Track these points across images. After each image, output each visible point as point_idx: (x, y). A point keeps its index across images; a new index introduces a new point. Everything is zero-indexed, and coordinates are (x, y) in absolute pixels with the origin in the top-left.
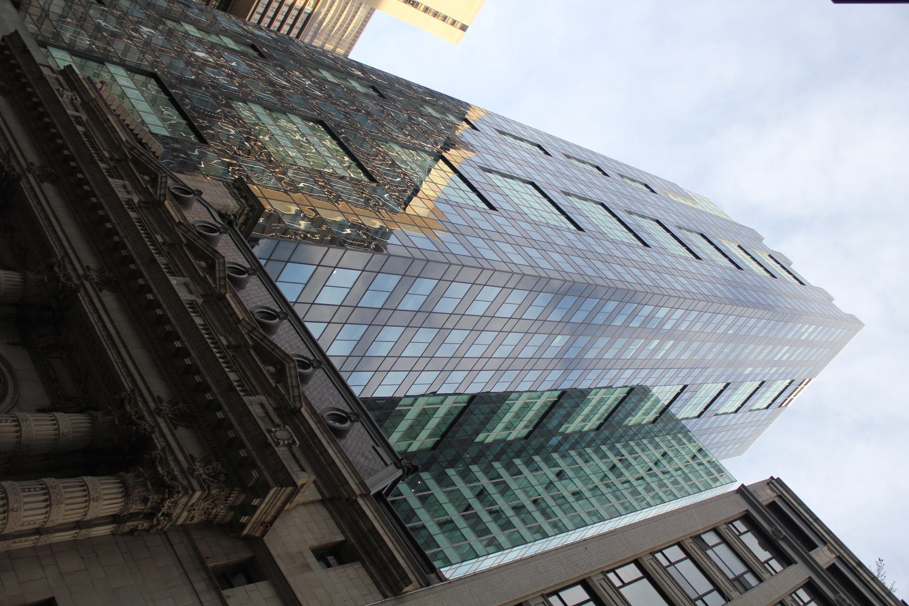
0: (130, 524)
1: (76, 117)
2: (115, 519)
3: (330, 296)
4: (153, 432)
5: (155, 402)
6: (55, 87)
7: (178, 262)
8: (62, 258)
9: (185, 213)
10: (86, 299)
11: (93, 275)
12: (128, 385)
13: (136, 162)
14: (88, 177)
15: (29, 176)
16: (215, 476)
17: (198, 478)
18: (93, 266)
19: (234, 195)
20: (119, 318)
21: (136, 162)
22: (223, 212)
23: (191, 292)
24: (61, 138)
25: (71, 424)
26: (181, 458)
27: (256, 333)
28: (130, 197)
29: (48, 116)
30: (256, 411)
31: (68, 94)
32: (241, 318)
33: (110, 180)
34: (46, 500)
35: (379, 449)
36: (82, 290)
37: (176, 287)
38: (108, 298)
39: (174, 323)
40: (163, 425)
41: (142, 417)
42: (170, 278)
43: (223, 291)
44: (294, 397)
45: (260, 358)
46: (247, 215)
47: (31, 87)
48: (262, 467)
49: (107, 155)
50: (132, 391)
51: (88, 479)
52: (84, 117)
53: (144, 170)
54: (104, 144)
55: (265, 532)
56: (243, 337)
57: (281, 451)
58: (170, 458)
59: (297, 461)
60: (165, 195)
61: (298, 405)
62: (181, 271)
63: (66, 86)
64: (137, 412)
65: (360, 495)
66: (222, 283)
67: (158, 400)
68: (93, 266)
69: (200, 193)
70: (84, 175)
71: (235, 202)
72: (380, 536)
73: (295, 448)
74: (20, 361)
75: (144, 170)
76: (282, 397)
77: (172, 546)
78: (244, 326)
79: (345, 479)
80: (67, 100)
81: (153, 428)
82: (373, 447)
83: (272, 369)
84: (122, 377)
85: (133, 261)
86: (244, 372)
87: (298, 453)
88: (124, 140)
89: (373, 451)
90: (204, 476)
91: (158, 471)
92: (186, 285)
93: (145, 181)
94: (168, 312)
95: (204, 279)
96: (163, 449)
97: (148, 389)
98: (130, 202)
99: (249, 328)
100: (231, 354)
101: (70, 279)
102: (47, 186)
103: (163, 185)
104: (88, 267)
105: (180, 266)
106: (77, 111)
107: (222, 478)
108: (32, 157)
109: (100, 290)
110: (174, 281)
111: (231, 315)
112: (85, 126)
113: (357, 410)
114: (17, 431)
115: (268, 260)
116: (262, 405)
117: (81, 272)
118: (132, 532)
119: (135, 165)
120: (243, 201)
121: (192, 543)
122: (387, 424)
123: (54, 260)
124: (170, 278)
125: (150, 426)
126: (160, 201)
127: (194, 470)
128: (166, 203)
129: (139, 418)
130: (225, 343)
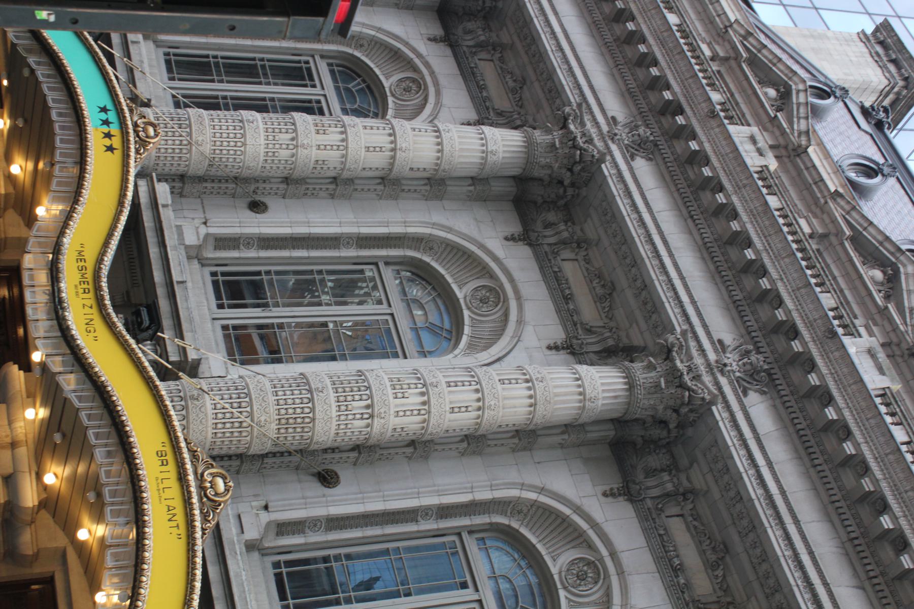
7: (836, 273)
10: (725, 415)
11: (732, 359)
13: (753, 62)
15: (614, 147)
18: (729, 339)
19: (875, 56)
20: (779, 450)
21: (753, 62)
23: (881, 371)
29: (633, 18)
33: (732, 129)
37: (856, 361)
38: (760, 409)
39: (879, 475)
46: (898, 93)
53: (767, 77)
54: (704, 35)
68: (729, 339)
69: (845, 91)
70: (700, 143)
75: (767, 77)
84: (795, 589)
88: (733, 20)
92: (871, 353)
93: (769, 99)
94: (865, 448)
101: (697, 378)
102: (640, 164)
104: (720, 342)
108: (615, 107)
109: (745, 394)
110: (852, 346)
112: (681, 16)
117: (712, 356)
120: (892, 68)
123: (671, 339)
124: (847, 340)
126: (800, 146)
128: (810, 150)
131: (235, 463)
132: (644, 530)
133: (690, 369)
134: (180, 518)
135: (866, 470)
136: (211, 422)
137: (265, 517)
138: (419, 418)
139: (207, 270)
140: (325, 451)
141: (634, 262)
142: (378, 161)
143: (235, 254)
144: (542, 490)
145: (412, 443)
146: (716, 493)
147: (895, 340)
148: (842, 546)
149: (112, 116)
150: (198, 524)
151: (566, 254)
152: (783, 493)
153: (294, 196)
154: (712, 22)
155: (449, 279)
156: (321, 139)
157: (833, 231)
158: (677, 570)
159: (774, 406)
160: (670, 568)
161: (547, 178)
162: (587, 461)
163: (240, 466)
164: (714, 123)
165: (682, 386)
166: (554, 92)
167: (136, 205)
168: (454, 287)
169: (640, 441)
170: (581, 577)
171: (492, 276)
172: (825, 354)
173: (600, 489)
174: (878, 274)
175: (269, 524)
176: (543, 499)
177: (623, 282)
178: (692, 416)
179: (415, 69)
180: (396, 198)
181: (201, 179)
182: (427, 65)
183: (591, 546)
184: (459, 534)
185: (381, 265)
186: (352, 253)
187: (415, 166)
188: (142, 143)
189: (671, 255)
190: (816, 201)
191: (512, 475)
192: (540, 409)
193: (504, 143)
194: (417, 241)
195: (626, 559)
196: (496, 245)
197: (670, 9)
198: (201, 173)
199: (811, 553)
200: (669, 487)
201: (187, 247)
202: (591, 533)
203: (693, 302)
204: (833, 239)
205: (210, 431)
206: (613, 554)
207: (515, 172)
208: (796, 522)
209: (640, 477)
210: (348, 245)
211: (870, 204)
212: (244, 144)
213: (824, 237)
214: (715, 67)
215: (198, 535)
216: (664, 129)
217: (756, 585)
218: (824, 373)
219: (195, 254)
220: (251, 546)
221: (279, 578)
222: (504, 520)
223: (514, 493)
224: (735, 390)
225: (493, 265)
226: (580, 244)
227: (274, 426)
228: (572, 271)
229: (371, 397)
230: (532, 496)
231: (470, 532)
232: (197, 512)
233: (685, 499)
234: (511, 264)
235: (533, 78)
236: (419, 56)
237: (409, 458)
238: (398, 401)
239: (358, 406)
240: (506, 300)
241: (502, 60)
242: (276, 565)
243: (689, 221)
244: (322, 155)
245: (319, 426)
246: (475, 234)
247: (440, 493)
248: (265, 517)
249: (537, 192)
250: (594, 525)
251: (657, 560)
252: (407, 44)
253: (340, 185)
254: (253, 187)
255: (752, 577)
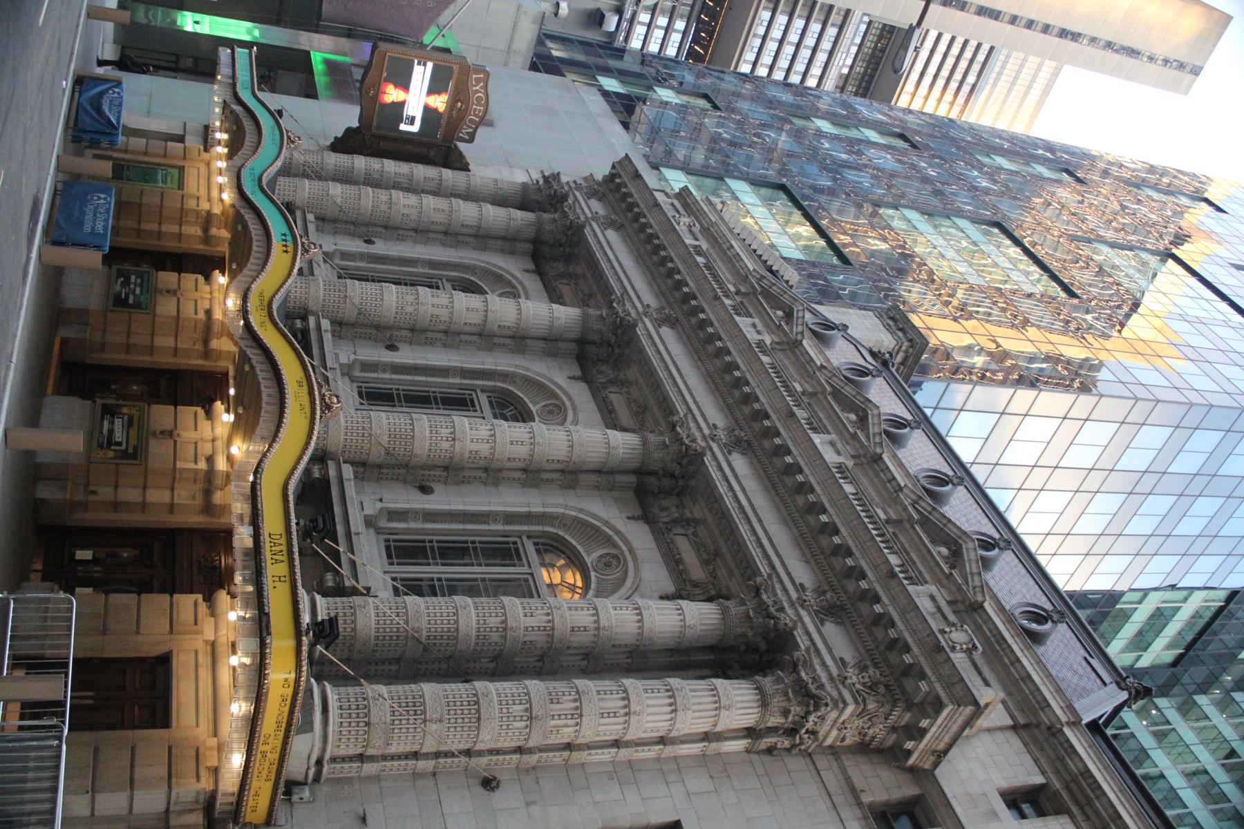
0: (767, 741)
1: (695, 247)
2: (751, 733)
3: (1022, 453)
4: (794, 628)
5: (797, 590)
6: (670, 213)
7: (821, 416)
8: (685, 415)
9: (828, 353)
10: (714, 463)
11: (721, 434)
12: (764, 569)
14: (712, 316)
16: (873, 687)
17: (850, 688)
18: (721, 423)
19: (888, 328)
21: (767, 294)
22: (875, 350)
23: (839, 453)
24: (679, 272)
25: (699, 616)
26: (829, 662)
27: (923, 504)
28: (760, 337)
29: (665, 249)
30: (925, 605)
31: (685, 220)
32: (902, 484)
33: (737, 318)
34: (671, 705)
35: (1094, 662)
36: (709, 453)
37: (819, 447)
38: (740, 462)
40: (807, 619)
41: (782, 609)
42: (813, 436)
43: (878, 451)
44: (974, 588)
45: (929, 536)
46: (906, 352)
47: (645, 216)
48: (933, 678)
49: (732, 289)
50: (770, 576)
51: (718, 682)
52: (704, 246)
53: (775, 302)
54: (729, 276)
55: (936, 764)
56: (906, 509)
57: (959, 658)
58: (816, 661)
59: (980, 673)
60: (802, 333)
61: (980, 598)
62: (825, 427)
63: (683, 212)
64: (775, 602)
65: (1067, 723)
66: (877, 440)
67: (801, 588)
69: (845, 327)
71: (890, 336)
72: (1096, 781)
73: (977, 656)
74: (639, 537)
75: (775, 302)
76: (959, 589)
77: (818, 771)
78: (906, 495)
79: (1045, 700)
80: (684, 228)
81: (795, 623)
82: (1085, 659)
83: (944, 551)
85: (767, 417)
86: (908, 554)
87: (980, 662)
89: (1084, 663)
90: (858, 686)
91: (800, 677)
92: (832, 443)
95: (854, 436)
96: (808, 650)
97: (789, 574)
98: (760, 344)
99: (914, 497)
100: (891, 530)
101: (694, 441)
102: (666, 331)
103: (800, 321)
105: (824, 420)
106: (697, 239)
107: (882, 689)
108: (649, 299)
109: (729, 452)
110: (817, 439)
111: (889, 481)
113: (1060, 606)
114: (639, 621)
115: (935, 408)
116: (932, 598)
117: (707, 431)
118: (770, 751)
119: (765, 298)
120: (900, 334)
121: (844, 771)
122: (1104, 627)
123: (676, 418)
124: (813, 436)
125: (791, 620)
127: (846, 678)
128: (804, 342)
129: (777, 610)
130: (883, 516)
131: (361, 469)
132: (656, 539)
133: (688, 436)
134: (308, 409)
135: (812, 490)
136: (343, 431)
137: (379, 505)
138: (488, 445)
139: (355, 385)
140: (423, 468)
141: (656, 386)
142: (475, 318)
143: (375, 375)
144: (581, 510)
145: (486, 470)
146: (710, 520)
147: (862, 452)
148: (796, 539)
149: (289, 238)
150: (318, 412)
151: (613, 389)
152: (752, 505)
153: (419, 344)
154: (739, 274)
155: (526, 400)
156: (435, 301)
157: (819, 389)
158: (679, 561)
159: (752, 463)
160: (673, 561)
161: (598, 341)
162: (616, 499)
163: (363, 473)
164: (717, 303)
165: (682, 444)
166: (607, 291)
167: (310, 356)
168: (530, 405)
169: (656, 490)
170: (608, 565)
171: (557, 397)
172: (787, 428)
173: (624, 515)
174: (853, 417)
175: (382, 509)
176: (581, 516)
177: (652, 402)
178: (691, 468)
179: (514, 287)
180: (490, 350)
181: (353, 325)
182: (521, 283)
183: (616, 546)
184: (520, 537)
185: (479, 391)
186: (458, 381)
187: (502, 324)
188: (307, 251)
189: (682, 377)
190: (807, 371)
191: (561, 500)
192: (576, 449)
193: (566, 315)
194: (505, 376)
195: (639, 553)
196: (561, 379)
197: (700, 255)
198: (352, 320)
199: (770, 539)
200: (676, 515)
201: (341, 365)
202: (615, 537)
203: (696, 402)
204: (820, 396)
205: (342, 437)
206: (631, 550)
207: (575, 335)
208: (760, 521)
209: (656, 510)
210: (455, 376)
211: (903, 450)
212: (382, 300)
213: (814, 394)
214: (738, 299)
215: (318, 417)
216: (682, 308)
217: (736, 571)
218: (797, 456)
219: (347, 371)
220: (369, 522)
221: (388, 548)
222: (555, 531)
223: (562, 511)
224: (721, 450)
225: (558, 391)
226: (623, 384)
227: (386, 438)
228: (617, 400)
229: (454, 427)
230: (574, 514)
231: (529, 537)
232: (318, 408)
233: (688, 524)
234: (570, 391)
235: (595, 289)
236: (516, 278)
237: (485, 484)
238: (474, 432)
239: (445, 432)
240: (566, 410)
241: (576, 284)
242: (387, 540)
243: (700, 364)
244: (436, 311)
245: (416, 443)
246: (546, 373)
247: (504, 504)
248: (379, 505)
249: (592, 350)
250: (618, 533)
251: (664, 556)
252: (507, 272)
253: (449, 336)
254: (388, 335)
255: (732, 565)
